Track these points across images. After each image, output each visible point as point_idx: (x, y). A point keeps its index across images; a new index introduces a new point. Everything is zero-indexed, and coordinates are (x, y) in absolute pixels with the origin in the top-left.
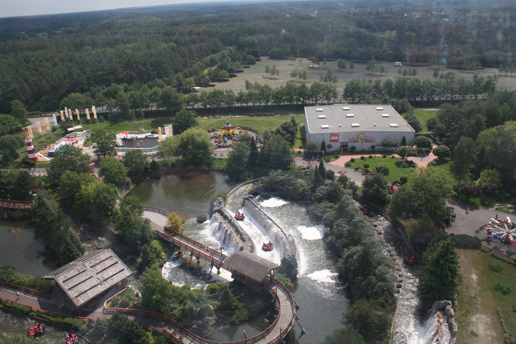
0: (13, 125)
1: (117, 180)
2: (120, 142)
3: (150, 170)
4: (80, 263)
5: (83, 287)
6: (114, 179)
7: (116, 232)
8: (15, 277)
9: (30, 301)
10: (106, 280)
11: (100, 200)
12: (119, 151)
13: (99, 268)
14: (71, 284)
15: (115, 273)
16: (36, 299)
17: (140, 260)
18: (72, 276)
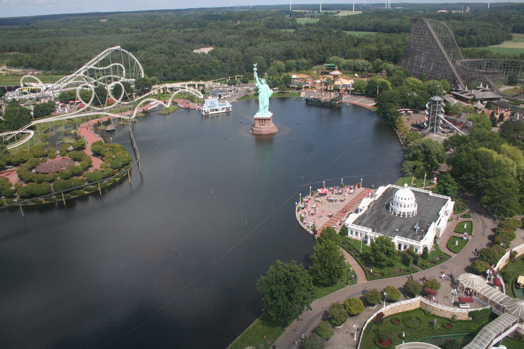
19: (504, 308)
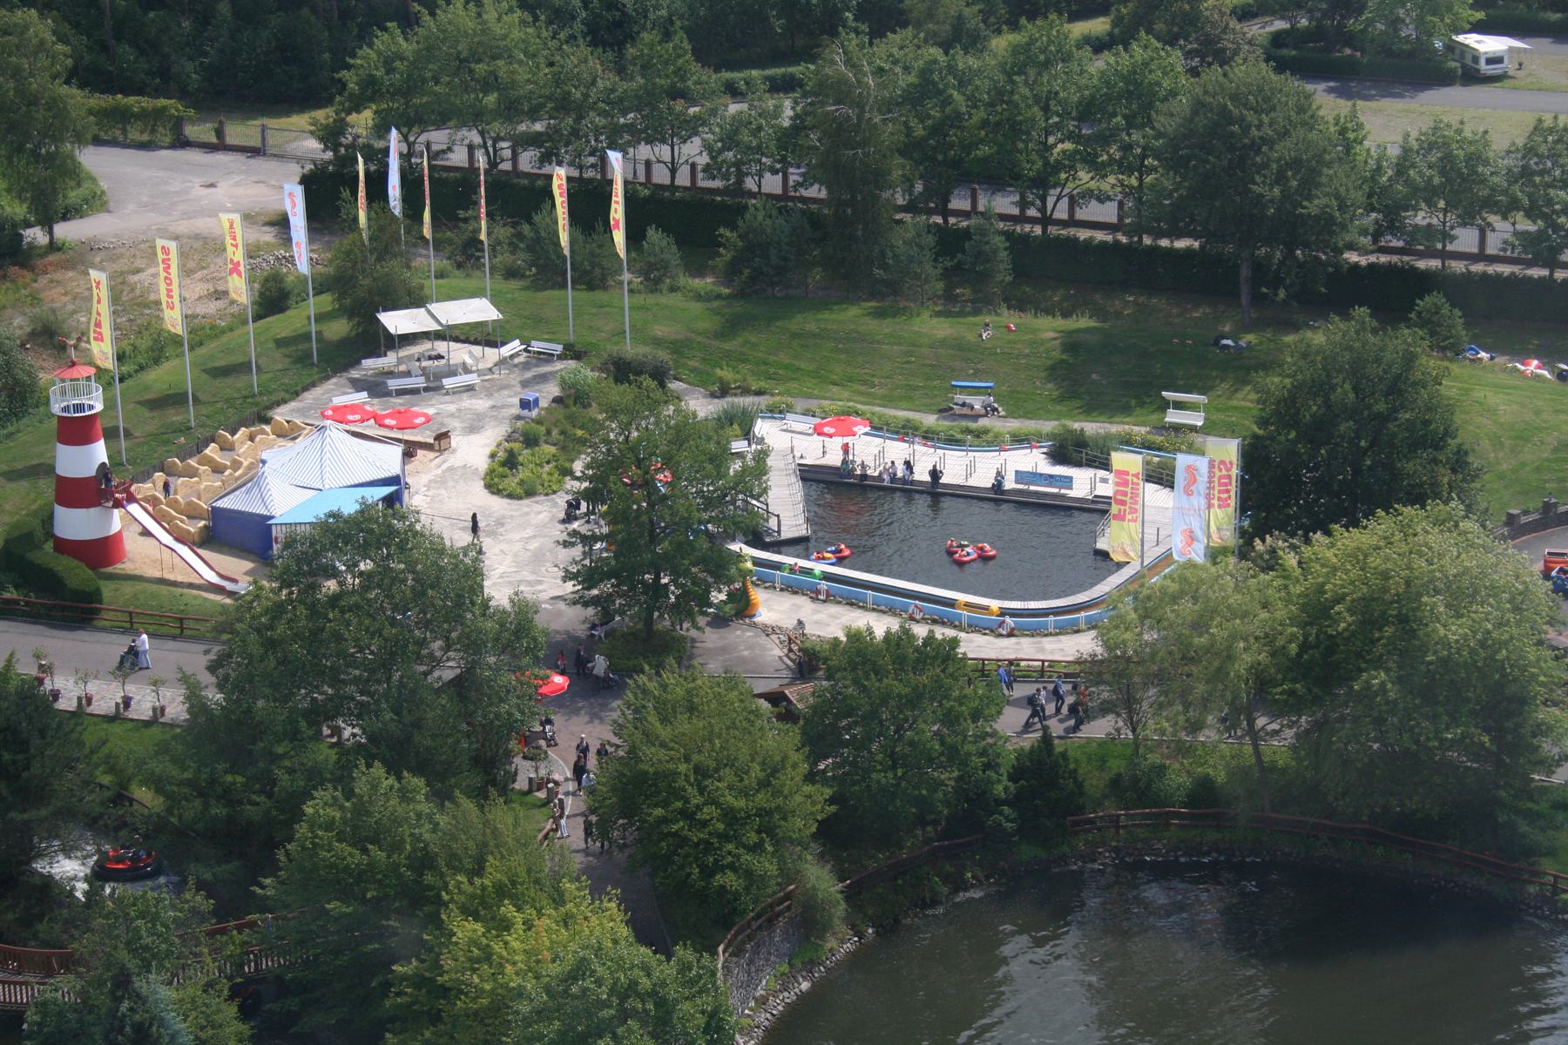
1: (730, 880)
2: (786, 506)
3: (1006, 819)
6: (708, 873)
12: (765, 583)
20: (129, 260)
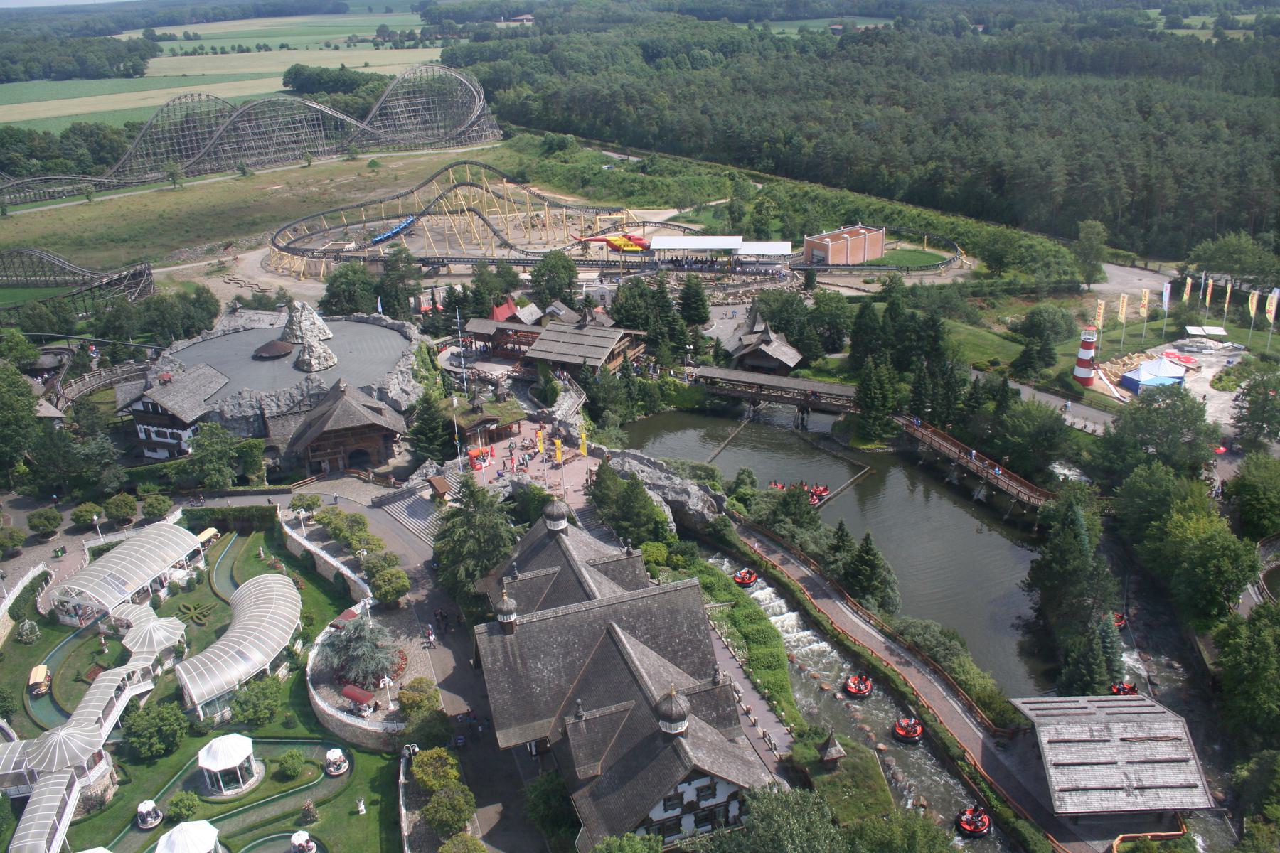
0: (1065, 273)
1: (1266, 522)
4: (1101, 714)
5: (1084, 777)
6: (1260, 518)
7: (1212, 668)
8: (960, 665)
9: (967, 734)
10: (1142, 788)
11: (1206, 572)
13: (1139, 751)
14: (1064, 755)
15: (1170, 783)
16: (981, 736)
17: (1245, 773)
18: (1073, 738)
19: (31, 773)
20: (1112, 298)
